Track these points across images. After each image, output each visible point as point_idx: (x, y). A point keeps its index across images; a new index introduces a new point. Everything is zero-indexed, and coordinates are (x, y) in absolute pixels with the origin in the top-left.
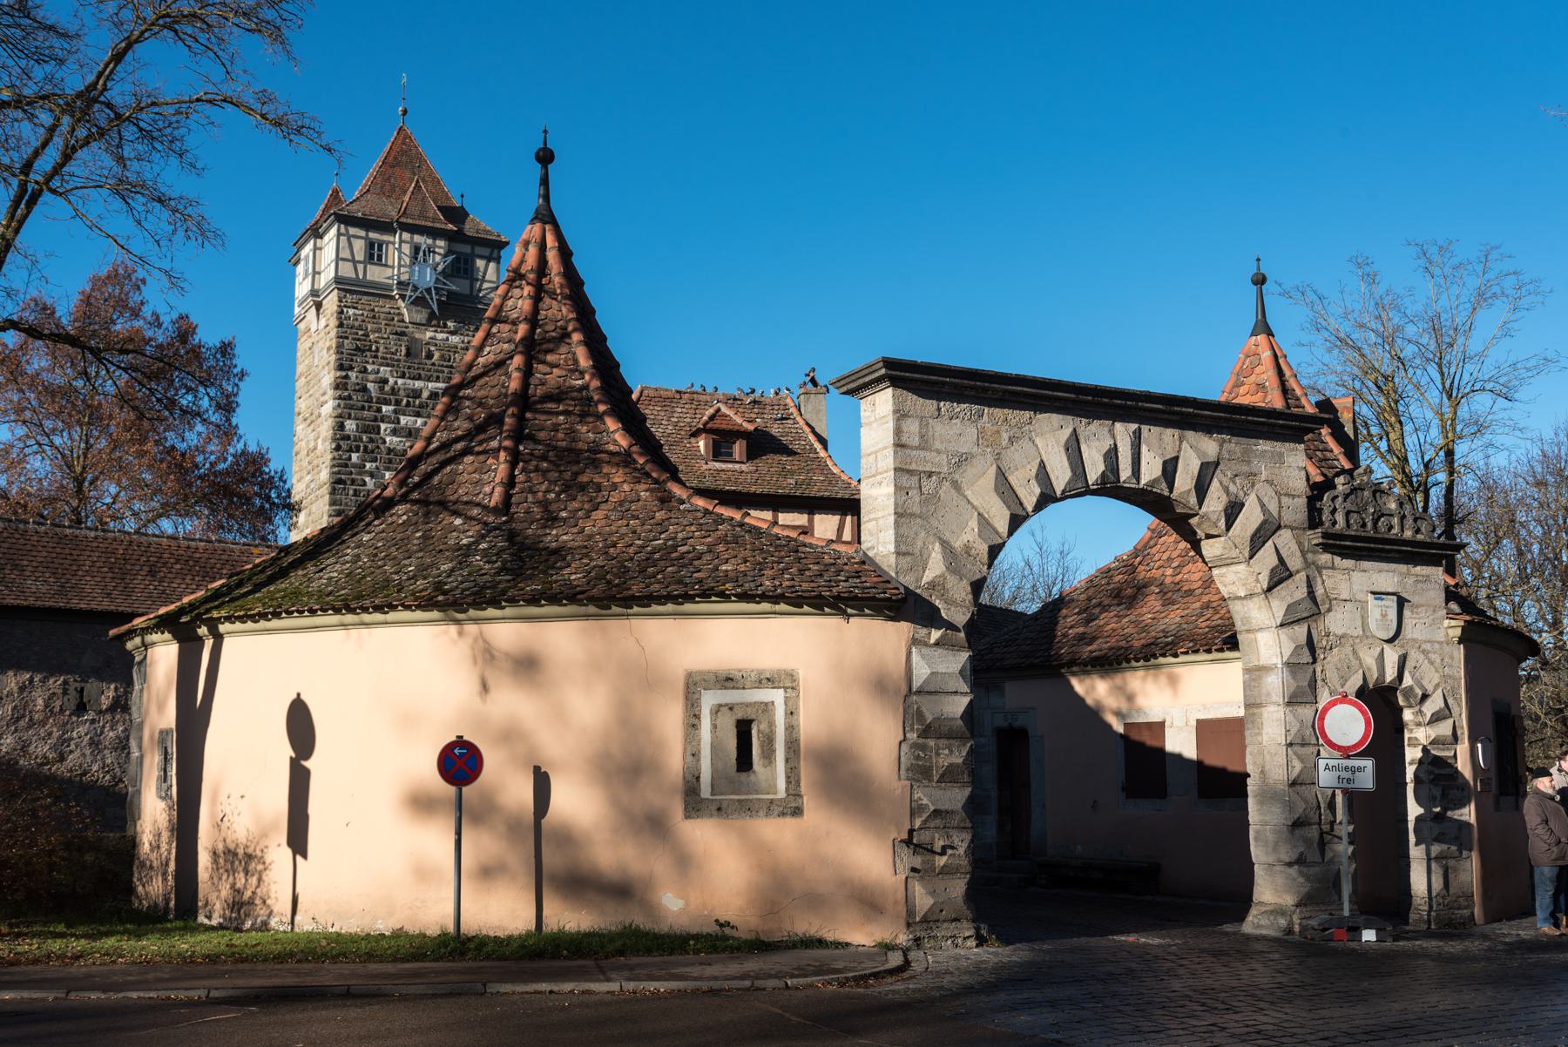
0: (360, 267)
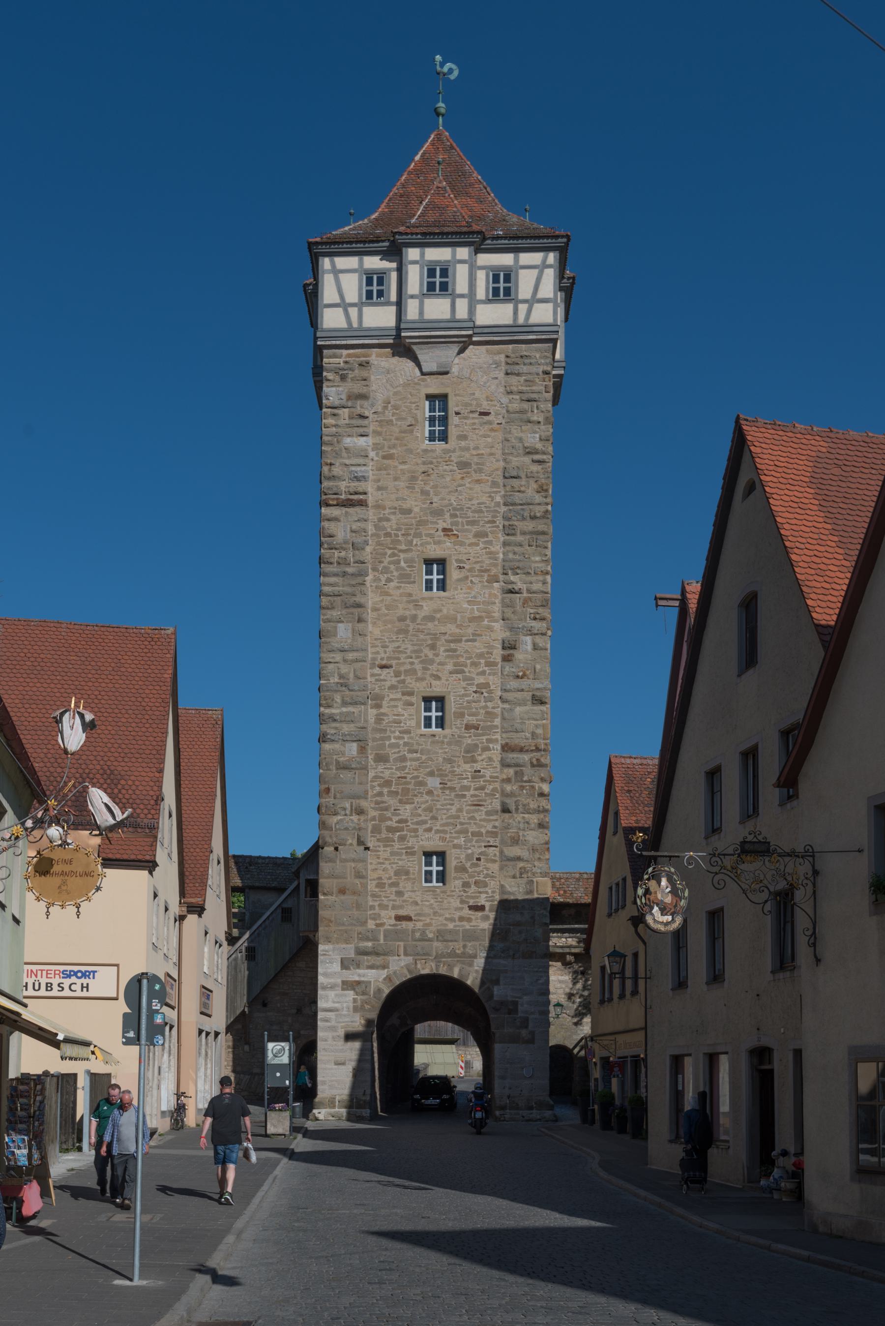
0: (353, 312)
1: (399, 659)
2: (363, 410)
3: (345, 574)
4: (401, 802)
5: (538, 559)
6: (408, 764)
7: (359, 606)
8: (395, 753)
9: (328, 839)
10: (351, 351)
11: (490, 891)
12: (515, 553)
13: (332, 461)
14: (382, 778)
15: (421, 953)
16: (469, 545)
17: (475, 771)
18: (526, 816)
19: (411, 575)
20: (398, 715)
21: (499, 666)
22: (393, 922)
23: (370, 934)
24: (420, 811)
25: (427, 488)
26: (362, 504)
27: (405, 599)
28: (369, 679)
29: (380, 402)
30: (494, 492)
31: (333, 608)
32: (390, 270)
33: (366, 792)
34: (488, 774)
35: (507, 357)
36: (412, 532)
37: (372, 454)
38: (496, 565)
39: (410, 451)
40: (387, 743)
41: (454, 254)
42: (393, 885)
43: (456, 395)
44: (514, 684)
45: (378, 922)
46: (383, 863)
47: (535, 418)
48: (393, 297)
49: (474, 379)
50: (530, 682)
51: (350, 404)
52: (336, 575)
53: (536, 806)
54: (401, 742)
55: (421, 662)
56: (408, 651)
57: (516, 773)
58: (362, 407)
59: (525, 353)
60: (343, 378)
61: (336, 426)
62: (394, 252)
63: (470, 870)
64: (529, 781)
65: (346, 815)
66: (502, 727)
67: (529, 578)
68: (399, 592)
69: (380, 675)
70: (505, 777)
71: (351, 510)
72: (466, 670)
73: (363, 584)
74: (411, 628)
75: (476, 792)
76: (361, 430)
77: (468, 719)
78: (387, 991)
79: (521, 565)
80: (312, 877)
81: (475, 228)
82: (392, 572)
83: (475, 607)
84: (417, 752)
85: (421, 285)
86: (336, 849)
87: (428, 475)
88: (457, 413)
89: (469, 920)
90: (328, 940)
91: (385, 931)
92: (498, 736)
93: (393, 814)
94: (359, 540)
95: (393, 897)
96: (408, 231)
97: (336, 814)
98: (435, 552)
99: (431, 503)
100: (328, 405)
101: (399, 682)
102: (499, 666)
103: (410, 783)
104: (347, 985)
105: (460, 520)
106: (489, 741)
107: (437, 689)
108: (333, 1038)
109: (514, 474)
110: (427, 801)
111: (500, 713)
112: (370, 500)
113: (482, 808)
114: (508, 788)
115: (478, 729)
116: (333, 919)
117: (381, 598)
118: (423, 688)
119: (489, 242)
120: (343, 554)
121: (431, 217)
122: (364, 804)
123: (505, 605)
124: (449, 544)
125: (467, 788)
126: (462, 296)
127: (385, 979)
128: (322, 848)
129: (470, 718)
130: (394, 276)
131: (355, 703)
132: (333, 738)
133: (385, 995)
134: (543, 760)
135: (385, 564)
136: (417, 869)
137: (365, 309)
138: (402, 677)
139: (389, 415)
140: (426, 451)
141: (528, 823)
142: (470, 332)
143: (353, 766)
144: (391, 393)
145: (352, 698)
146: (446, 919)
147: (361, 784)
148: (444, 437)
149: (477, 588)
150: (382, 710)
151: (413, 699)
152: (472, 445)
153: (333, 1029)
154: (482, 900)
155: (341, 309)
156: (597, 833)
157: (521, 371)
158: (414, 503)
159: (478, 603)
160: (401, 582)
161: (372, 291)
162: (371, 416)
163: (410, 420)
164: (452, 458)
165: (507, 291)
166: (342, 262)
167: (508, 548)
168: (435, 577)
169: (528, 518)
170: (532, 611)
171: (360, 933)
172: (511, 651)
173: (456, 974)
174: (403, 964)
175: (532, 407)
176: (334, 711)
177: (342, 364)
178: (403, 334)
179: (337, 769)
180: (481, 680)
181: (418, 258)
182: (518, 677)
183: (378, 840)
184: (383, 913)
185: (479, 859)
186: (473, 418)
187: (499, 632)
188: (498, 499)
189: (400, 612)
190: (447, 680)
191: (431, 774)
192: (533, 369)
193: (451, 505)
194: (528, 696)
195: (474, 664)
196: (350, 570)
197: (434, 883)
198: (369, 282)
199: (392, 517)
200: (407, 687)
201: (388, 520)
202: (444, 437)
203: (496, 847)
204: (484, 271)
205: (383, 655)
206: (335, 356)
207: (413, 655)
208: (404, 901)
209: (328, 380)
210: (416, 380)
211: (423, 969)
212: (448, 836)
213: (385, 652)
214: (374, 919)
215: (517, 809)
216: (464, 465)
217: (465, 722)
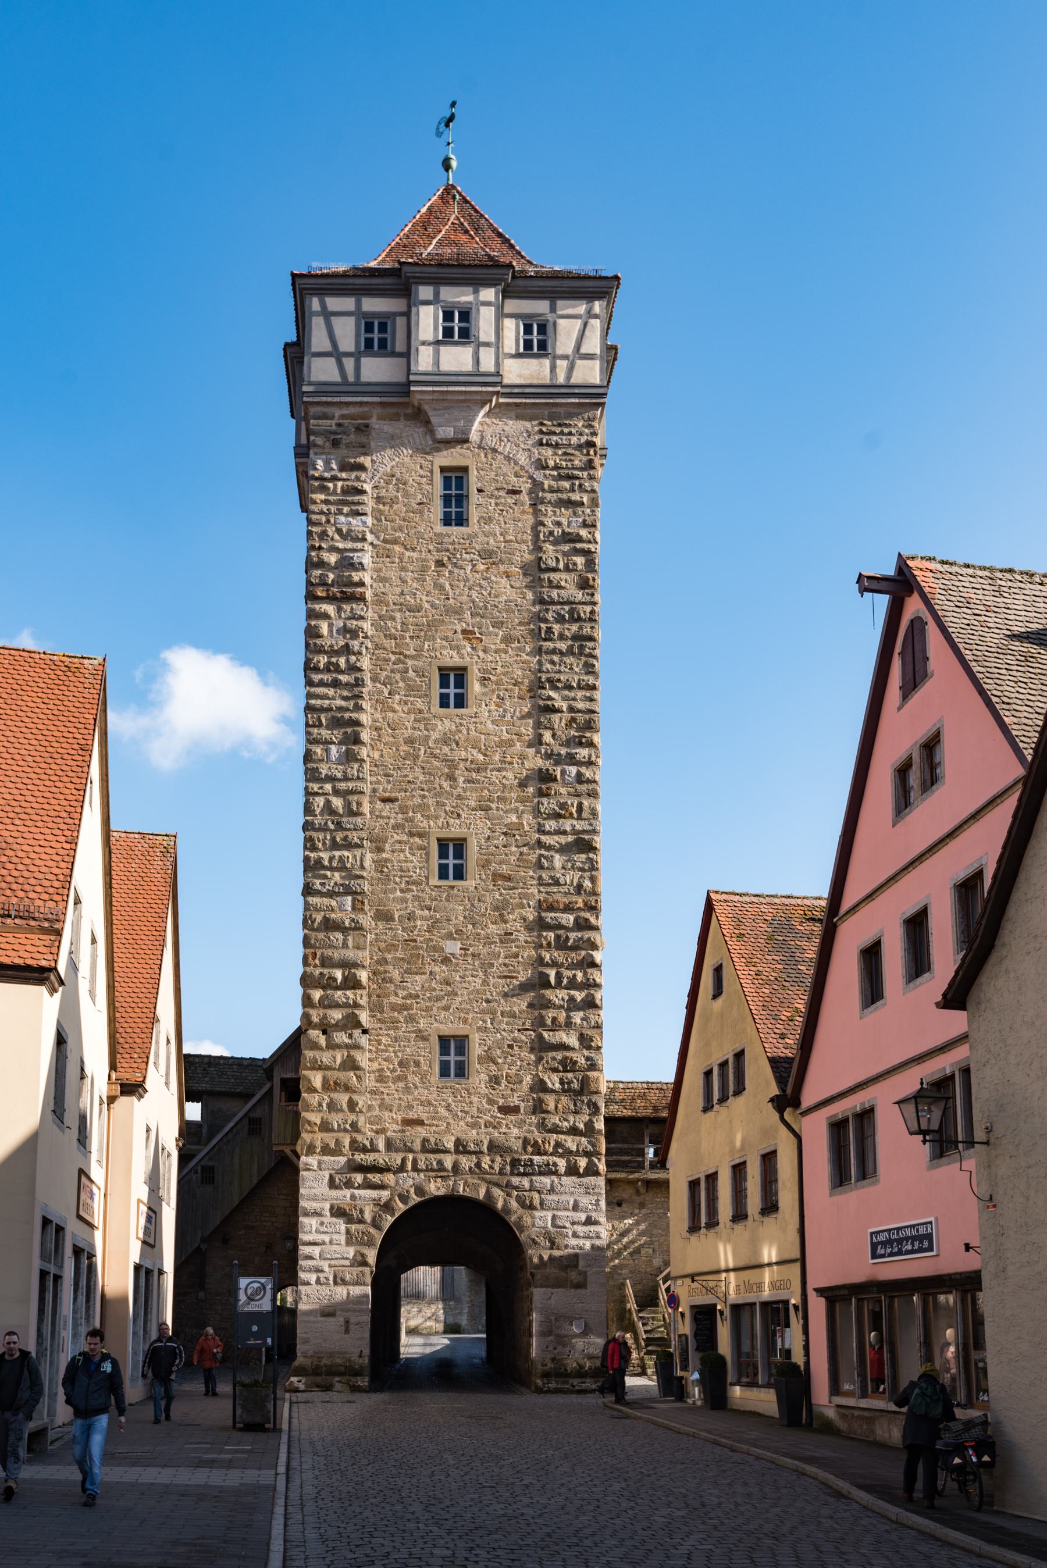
0: (349, 364)
10: (345, 411)
16: (496, 652)
17: (506, 934)
25: (442, 580)
32: (395, 314)
34: (522, 938)
39: (420, 536)
42: (399, 1079)
51: (344, 475)
54: (409, 896)
57: (558, 937)
60: (336, 443)
72: (493, 806)
75: (507, 961)
88: (480, 491)
98: (451, 659)
99: (448, 599)
104: (338, 1212)
107: (456, 830)
118: (436, 829)
126: (487, 344)
128: (306, 1030)
134: (593, 920)
147: (358, 948)
148: (461, 520)
150: (384, 855)
155: (332, 360)
156: (685, 1000)
158: (424, 598)
161: (372, 339)
165: (542, 345)
166: (334, 303)
175: (573, 484)
177: (334, 427)
178: (412, 389)
185: (511, 1047)
191: (450, 936)
196: (344, 678)
198: (369, 328)
199: (398, 615)
200: (418, 826)
201: (393, 619)
202: (461, 520)
206: (325, 417)
207: (426, 787)
209: (316, 446)
216: (487, 554)
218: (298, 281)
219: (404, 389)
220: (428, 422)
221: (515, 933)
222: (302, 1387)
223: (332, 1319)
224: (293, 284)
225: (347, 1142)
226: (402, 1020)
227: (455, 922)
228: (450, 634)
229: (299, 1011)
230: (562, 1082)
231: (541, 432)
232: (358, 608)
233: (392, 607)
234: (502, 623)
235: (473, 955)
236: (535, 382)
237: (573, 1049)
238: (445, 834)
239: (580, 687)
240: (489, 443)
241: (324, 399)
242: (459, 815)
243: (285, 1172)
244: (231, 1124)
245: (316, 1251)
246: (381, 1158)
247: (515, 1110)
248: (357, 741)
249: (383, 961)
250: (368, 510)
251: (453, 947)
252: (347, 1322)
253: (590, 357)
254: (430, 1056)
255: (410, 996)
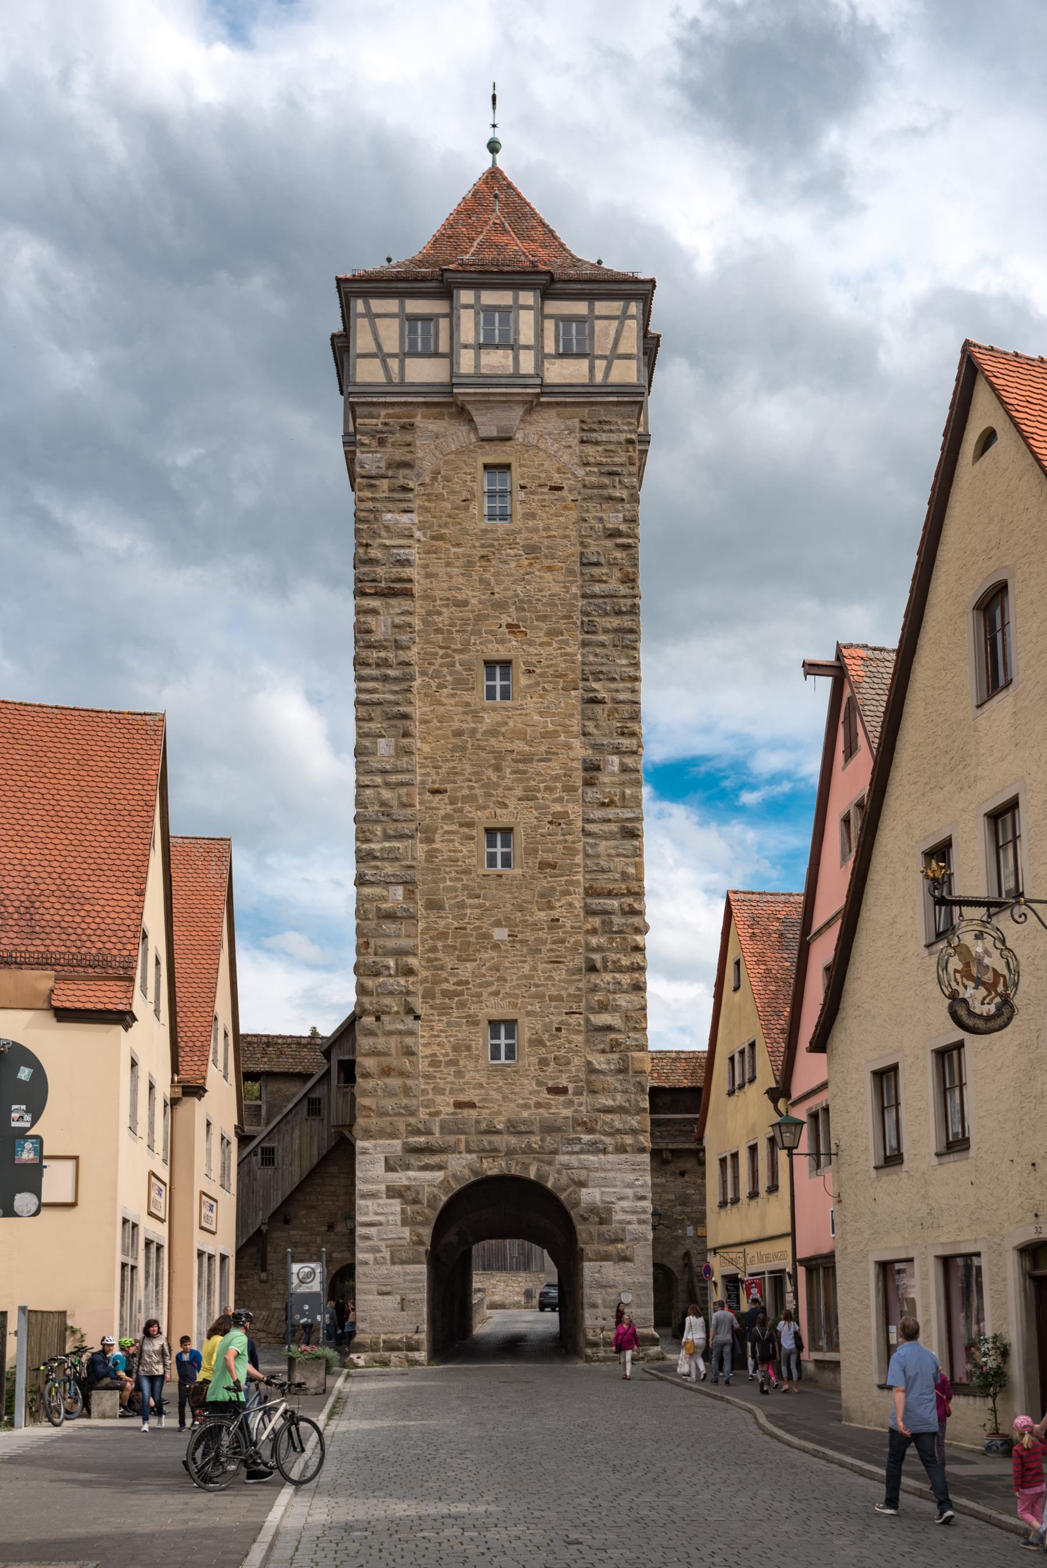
0: (394, 364)
1: (455, 782)
2: (406, 481)
3: (386, 679)
4: (459, 959)
5: (624, 662)
6: (468, 911)
7: (406, 717)
8: (451, 898)
9: (368, 1007)
10: (391, 411)
11: (573, 1069)
12: (596, 655)
13: (369, 542)
14: (436, 929)
15: (488, 1148)
16: (540, 645)
17: (553, 920)
18: (617, 975)
19: (468, 679)
20: (455, 851)
21: (580, 791)
22: (451, 1110)
23: (421, 1126)
24: (483, 970)
25: (487, 576)
26: (408, 594)
27: (460, 709)
28: (418, 807)
29: (427, 473)
30: (568, 582)
31: (371, 719)
33: (416, 946)
34: (569, 924)
35: (583, 422)
36: (469, 628)
37: (418, 534)
38: (573, 670)
39: (465, 532)
40: (442, 885)
41: (516, 299)
42: (453, 1063)
43: (521, 466)
44: (598, 814)
45: (432, 1110)
46: (438, 1036)
47: (618, 494)
48: (443, 347)
49: (543, 446)
50: (618, 811)
52: (374, 679)
53: (628, 963)
54: (459, 885)
55: (483, 786)
56: (466, 773)
57: (603, 922)
58: (403, 477)
59: (604, 418)
60: (382, 442)
61: (373, 499)
62: (446, 293)
63: (548, 1044)
64: (621, 932)
65: (390, 975)
66: (586, 866)
67: (614, 686)
68: (453, 701)
69: (431, 802)
70: (589, 927)
71: (393, 602)
72: (539, 795)
73: (408, 690)
74: (469, 745)
75: (554, 946)
76: (405, 505)
77: (542, 856)
78: (444, 1199)
79: (604, 669)
80: (346, 1058)
81: (542, 268)
82: (445, 676)
83: (549, 720)
84: (479, 897)
85: (477, 333)
86: (378, 1019)
87: (489, 560)
88: (523, 487)
89: (548, 1106)
90: (368, 1134)
91: (442, 1121)
92: (580, 877)
93: (451, 974)
94: (404, 638)
95: (451, 1079)
96: (460, 268)
97: (377, 974)
99: (493, 594)
100: (364, 473)
101: (455, 810)
102: (580, 791)
103: (471, 935)
104: (393, 1192)
105: (528, 614)
106: (569, 883)
107: (504, 818)
108: (375, 1259)
109: (595, 559)
110: (493, 958)
111: (581, 848)
112: (417, 589)
113: (561, 966)
114: (594, 941)
115: (554, 867)
116: (374, 1107)
117: (432, 708)
119: (559, 286)
120: (382, 654)
121: (488, 256)
122: (413, 962)
123: (586, 718)
124: (514, 643)
125: (544, 942)
127: (442, 1182)
128: (360, 1017)
129: (545, 855)
130: (444, 323)
131: (401, 837)
132: (373, 879)
133: (442, 1204)
134: (636, 906)
135: (436, 667)
136: (481, 1042)
137: (407, 361)
138: (459, 805)
139: (438, 488)
140: (485, 531)
141: (619, 983)
142: (538, 390)
143: (399, 914)
144: (441, 462)
145: (396, 830)
146: (519, 1106)
147: (409, 936)
149: (551, 696)
150: (434, 846)
151: (474, 832)
152: (541, 526)
153: (376, 1250)
154: (563, 1082)
157: (599, 439)
158: (470, 593)
159: (554, 715)
160: (457, 689)
162: (417, 489)
163: (465, 495)
164: (518, 540)
167: (587, 649)
168: (498, 683)
169: (612, 613)
170: (619, 725)
171: (410, 1125)
172: (595, 773)
173: (532, 1175)
174: (464, 1162)
176: (373, 846)
178: (455, 390)
179: (379, 918)
180: (558, 808)
181: (472, 302)
182: (603, 804)
183: (432, 1007)
184: (439, 1099)
185: (559, 1029)
186: (542, 493)
187: (580, 750)
188: (574, 589)
189: (456, 725)
190: (515, 808)
191: (498, 924)
192: (614, 437)
193: (517, 596)
194: (614, 827)
195: (549, 789)
196: (391, 673)
197: (503, 1060)
199: (444, 610)
201: (439, 613)
203: (580, 1013)
204: (553, 321)
205: (435, 777)
207: (473, 778)
208: (465, 1083)
209: (363, 445)
210: (471, 447)
211: (491, 1169)
212: (520, 1001)
213: (438, 774)
214: (427, 1106)
215: (605, 968)
216: (531, 549)
217: (539, 859)
218: (342, 286)
219: (448, 390)
220: (472, 420)
221: (561, 919)
222: (361, 1363)
223: (390, 1297)
224: (338, 287)
225: (402, 1127)
226: (454, 1006)
227: (503, 909)
228: (494, 628)
229: (354, 998)
230: (608, 1062)
231: (583, 430)
232: (406, 604)
233: (439, 602)
234: (546, 616)
235: (521, 941)
236: (575, 381)
237: (619, 1031)
238: (492, 824)
239: (623, 680)
240: (531, 440)
241: (370, 399)
242: (506, 806)
243: (340, 1154)
244: (291, 1106)
245: (372, 1231)
246: (437, 1138)
247: (564, 1091)
248: (406, 734)
249: (434, 949)
250: (414, 506)
251: (500, 934)
252: (403, 1300)
253: (627, 357)
254: (482, 1040)
255: (459, 983)
